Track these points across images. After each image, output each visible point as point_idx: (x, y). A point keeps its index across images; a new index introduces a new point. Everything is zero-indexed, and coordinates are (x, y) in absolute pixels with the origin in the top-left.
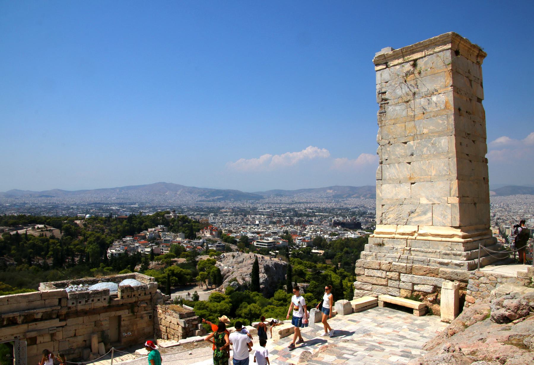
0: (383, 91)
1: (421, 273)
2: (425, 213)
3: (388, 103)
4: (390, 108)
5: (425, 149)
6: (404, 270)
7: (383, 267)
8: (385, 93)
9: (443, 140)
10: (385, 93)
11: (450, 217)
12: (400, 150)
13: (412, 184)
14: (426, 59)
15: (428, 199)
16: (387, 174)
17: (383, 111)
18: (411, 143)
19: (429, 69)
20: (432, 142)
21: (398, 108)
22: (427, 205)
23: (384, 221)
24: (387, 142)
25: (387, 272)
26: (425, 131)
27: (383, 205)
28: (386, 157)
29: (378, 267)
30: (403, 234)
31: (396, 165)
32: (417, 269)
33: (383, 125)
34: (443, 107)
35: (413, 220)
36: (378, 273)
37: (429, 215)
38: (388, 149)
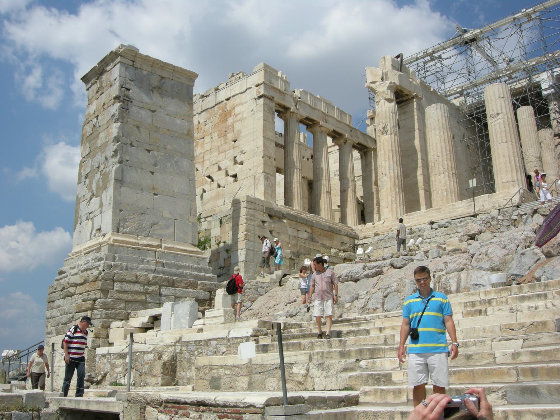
0: (127, 86)
1: (183, 285)
2: (167, 227)
3: (132, 102)
4: (134, 108)
5: (169, 164)
6: (166, 283)
7: (142, 279)
8: (129, 90)
9: (185, 162)
10: (129, 90)
11: (191, 235)
12: (143, 156)
13: (155, 194)
14: (172, 82)
15: (171, 214)
16: (128, 176)
17: (126, 107)
18: (155, 153)
19: (175, 93)
20: (175, 159)
21: (143, 112)
22: (170, 219)
23: (121, 229)
24: (129, 142)
25: (144, 285)
26: (169, 147)
27: (121, 211)
28: (128, 158)
29: (134, 278)
30: (148, 245)
31: (139, 170)
32: (178, 282)
33: (125, 121)
34: (186, 132)
35: (156, 232)
36: (137, 287)
37: (172, 229)
38: (130, 150)
